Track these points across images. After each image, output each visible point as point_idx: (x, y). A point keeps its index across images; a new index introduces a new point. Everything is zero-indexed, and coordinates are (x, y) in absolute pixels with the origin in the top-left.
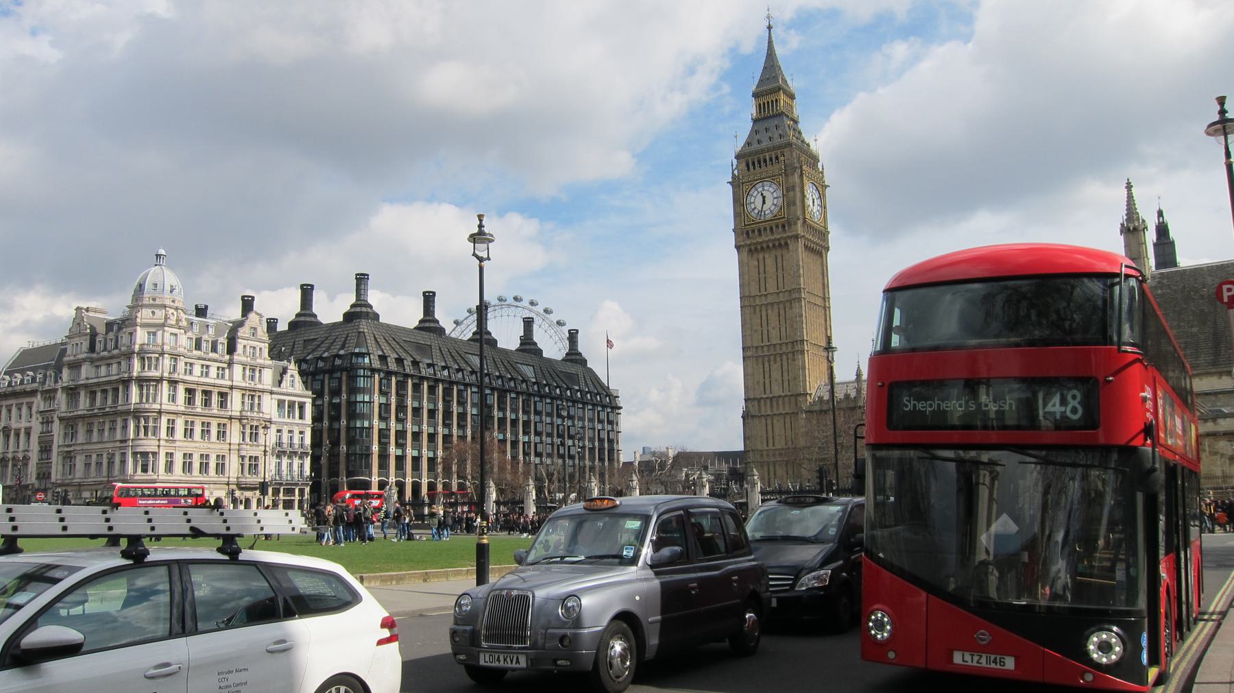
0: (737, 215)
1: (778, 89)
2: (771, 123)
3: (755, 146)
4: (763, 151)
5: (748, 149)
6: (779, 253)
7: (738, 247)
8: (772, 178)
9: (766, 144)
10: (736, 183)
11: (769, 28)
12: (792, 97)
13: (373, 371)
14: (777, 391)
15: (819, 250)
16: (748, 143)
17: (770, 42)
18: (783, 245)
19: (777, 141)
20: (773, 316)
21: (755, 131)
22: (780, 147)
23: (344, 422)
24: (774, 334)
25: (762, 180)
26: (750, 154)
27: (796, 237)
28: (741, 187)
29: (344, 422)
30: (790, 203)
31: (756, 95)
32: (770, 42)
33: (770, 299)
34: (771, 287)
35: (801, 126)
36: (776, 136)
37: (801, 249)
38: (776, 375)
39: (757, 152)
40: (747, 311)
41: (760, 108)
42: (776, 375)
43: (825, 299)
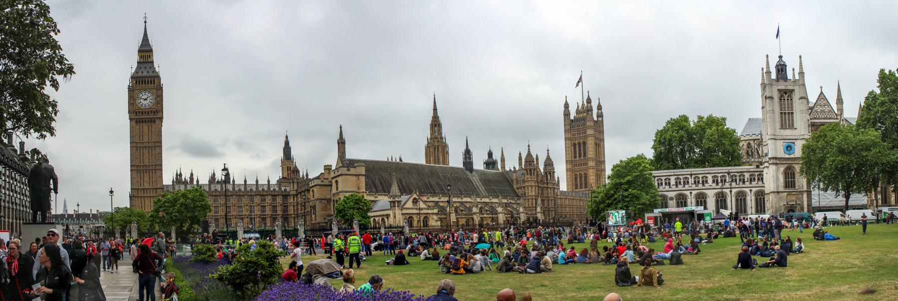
7: (131, 119)
8: (150, 90)
18: (152, 121)
25: (145, 90)
34: (146, 139)
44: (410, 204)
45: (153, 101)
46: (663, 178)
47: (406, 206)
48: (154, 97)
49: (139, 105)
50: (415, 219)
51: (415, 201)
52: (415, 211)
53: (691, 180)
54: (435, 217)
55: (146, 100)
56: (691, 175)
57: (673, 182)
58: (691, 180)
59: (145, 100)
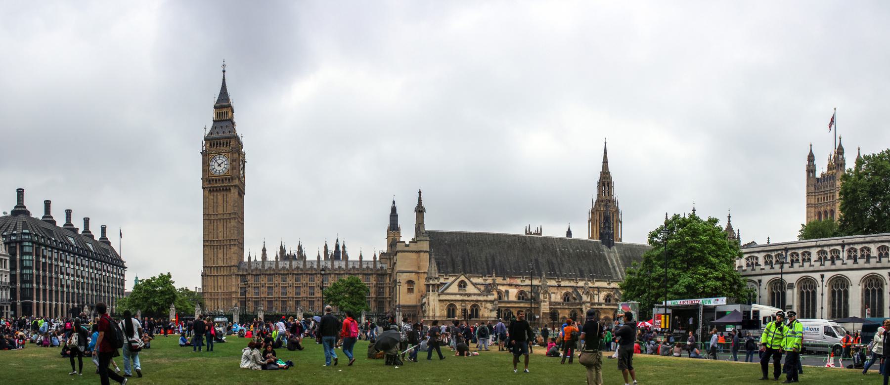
0: (204, 171)
1: (229, 106)
2: (224, 124)
3: (215, 136)
4: (219, 139)
5: (211, 136)
6: (225, 193)
7: (203, 188)
9: (221, 135)
10: (204, 154)
11: (224, 71)
12: (233, 112)
13: (33, 243)
14: (220, 263)
15: (241, 194)
16: (211, 133)
17: (224, 80)
18: (227, 189)
19: (228, 134)
20: (220, 225)
21: (214, 127)
22: (229, 138)
23: (18, 271)
24: (220, 234)
26: (212, 139)
27: (235, 186)
28: (206, 157)
29: (18, 271)
30: (233, 168)
31: (215, 107)
32: (224, 80)
33: (219, 217)
34: (220, 211)
35: (236, 128)
36: (227, 131)
37: (237, 193)
38: (220, 255)
39: (215, 139)
40: (208, 222)
41: (217, 114)
42: (220, 255)
43: (243, 219)
44: (454, 288)
45: (228, 167)
46: (800, 252)
47: (449, 291)
48: (228, 162)
49: (213, 172)
50: (459, 306)
51: (462, 285)
52: (458, 297)
53: (844, 255)
54: (489, 306)
55: (221, 165)
56: (843, 246)
57: (874, 252)
58: (844, 255)
59: (219, 165)
